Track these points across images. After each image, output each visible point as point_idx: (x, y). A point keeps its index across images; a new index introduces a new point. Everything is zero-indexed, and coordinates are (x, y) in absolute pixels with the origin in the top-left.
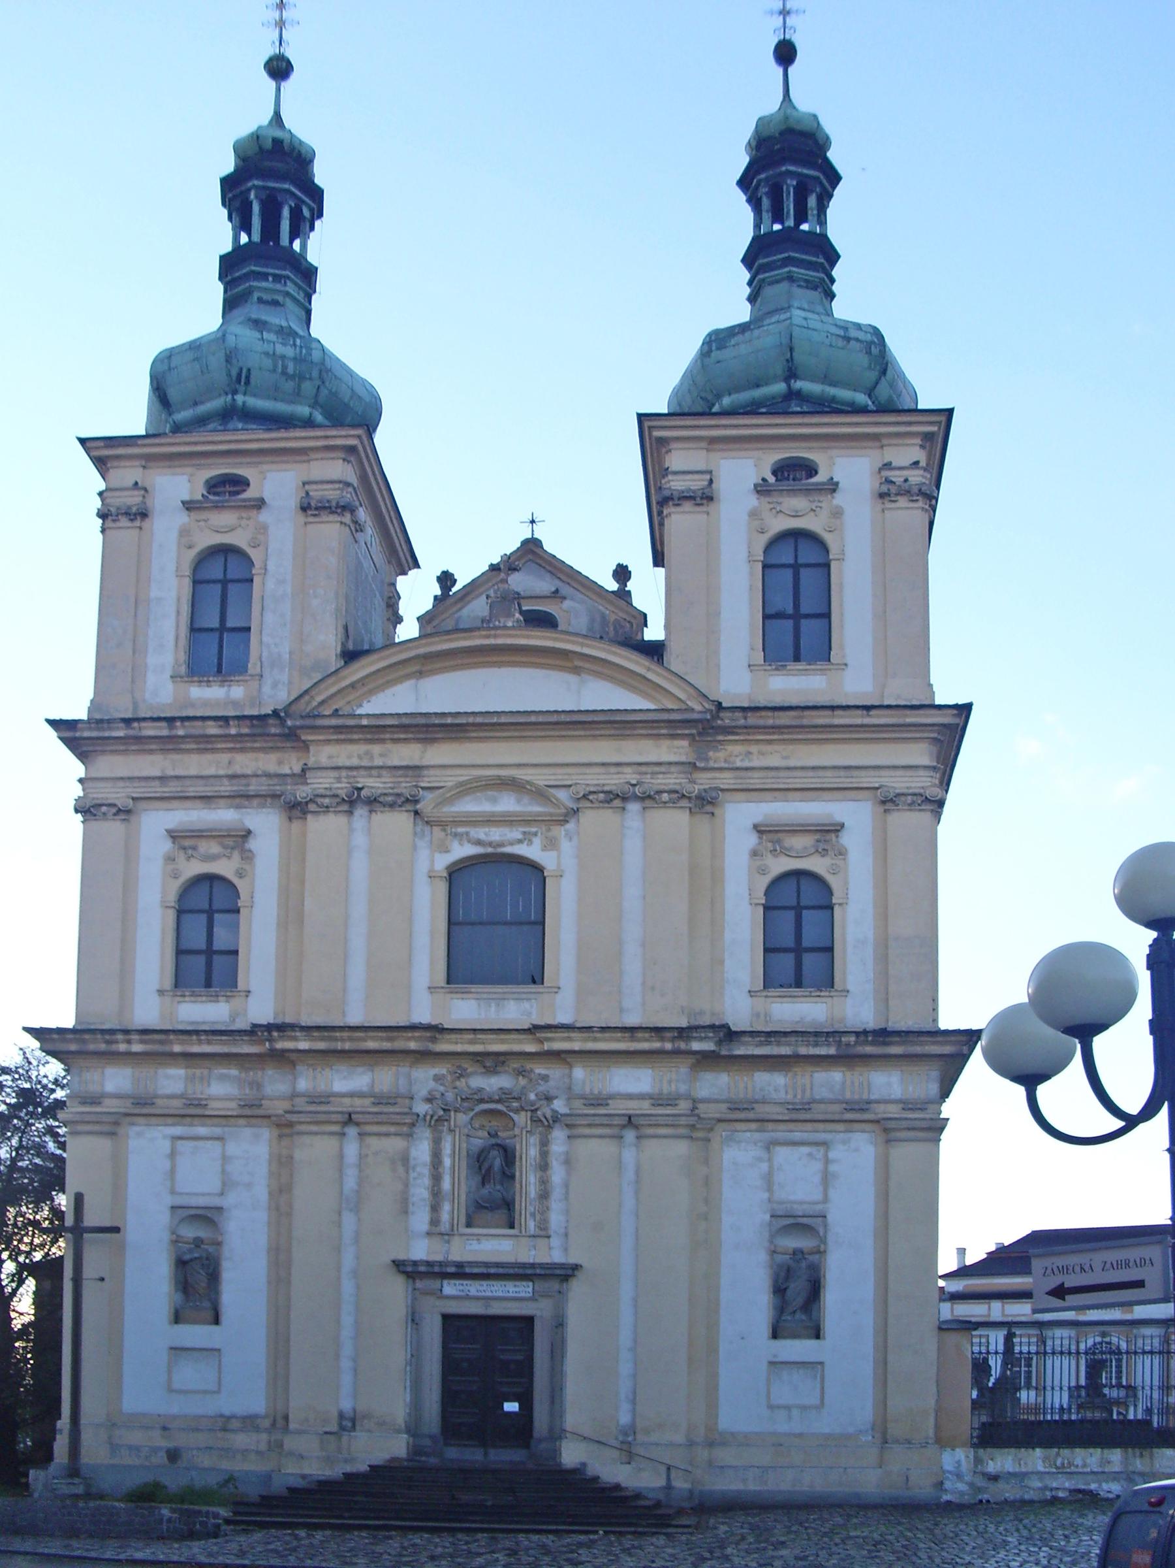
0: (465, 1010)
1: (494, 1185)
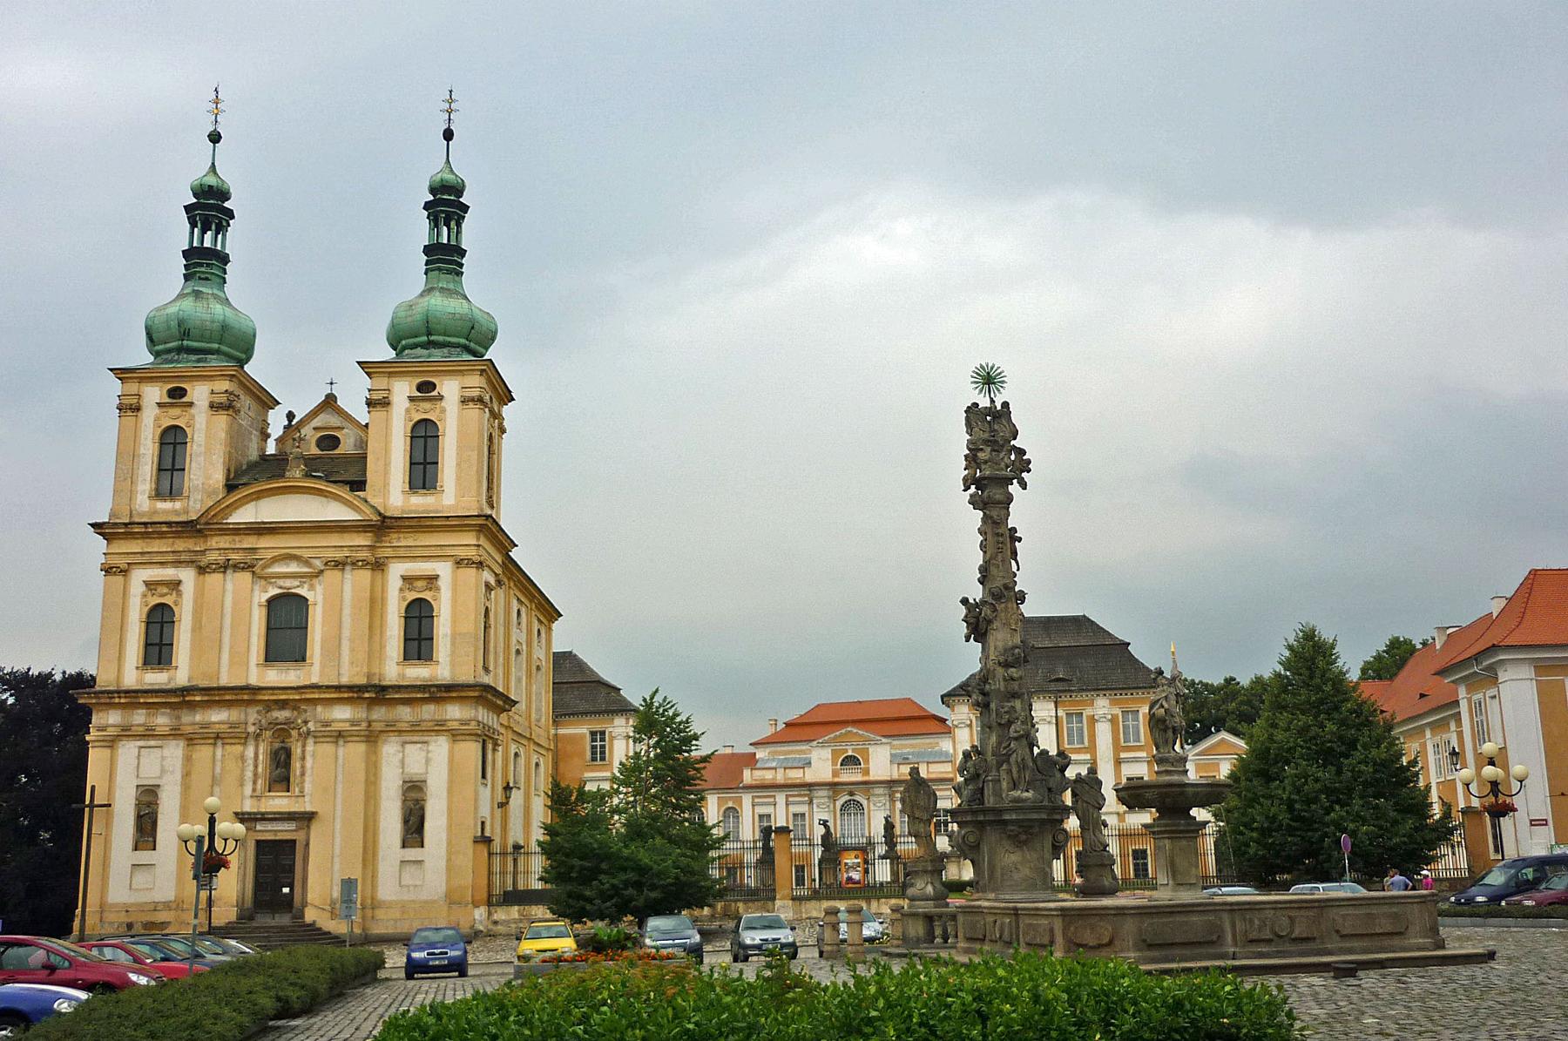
0: (277, 676)
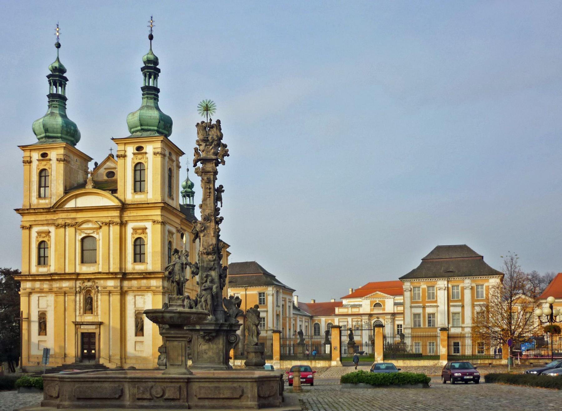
1: (89, 306)
